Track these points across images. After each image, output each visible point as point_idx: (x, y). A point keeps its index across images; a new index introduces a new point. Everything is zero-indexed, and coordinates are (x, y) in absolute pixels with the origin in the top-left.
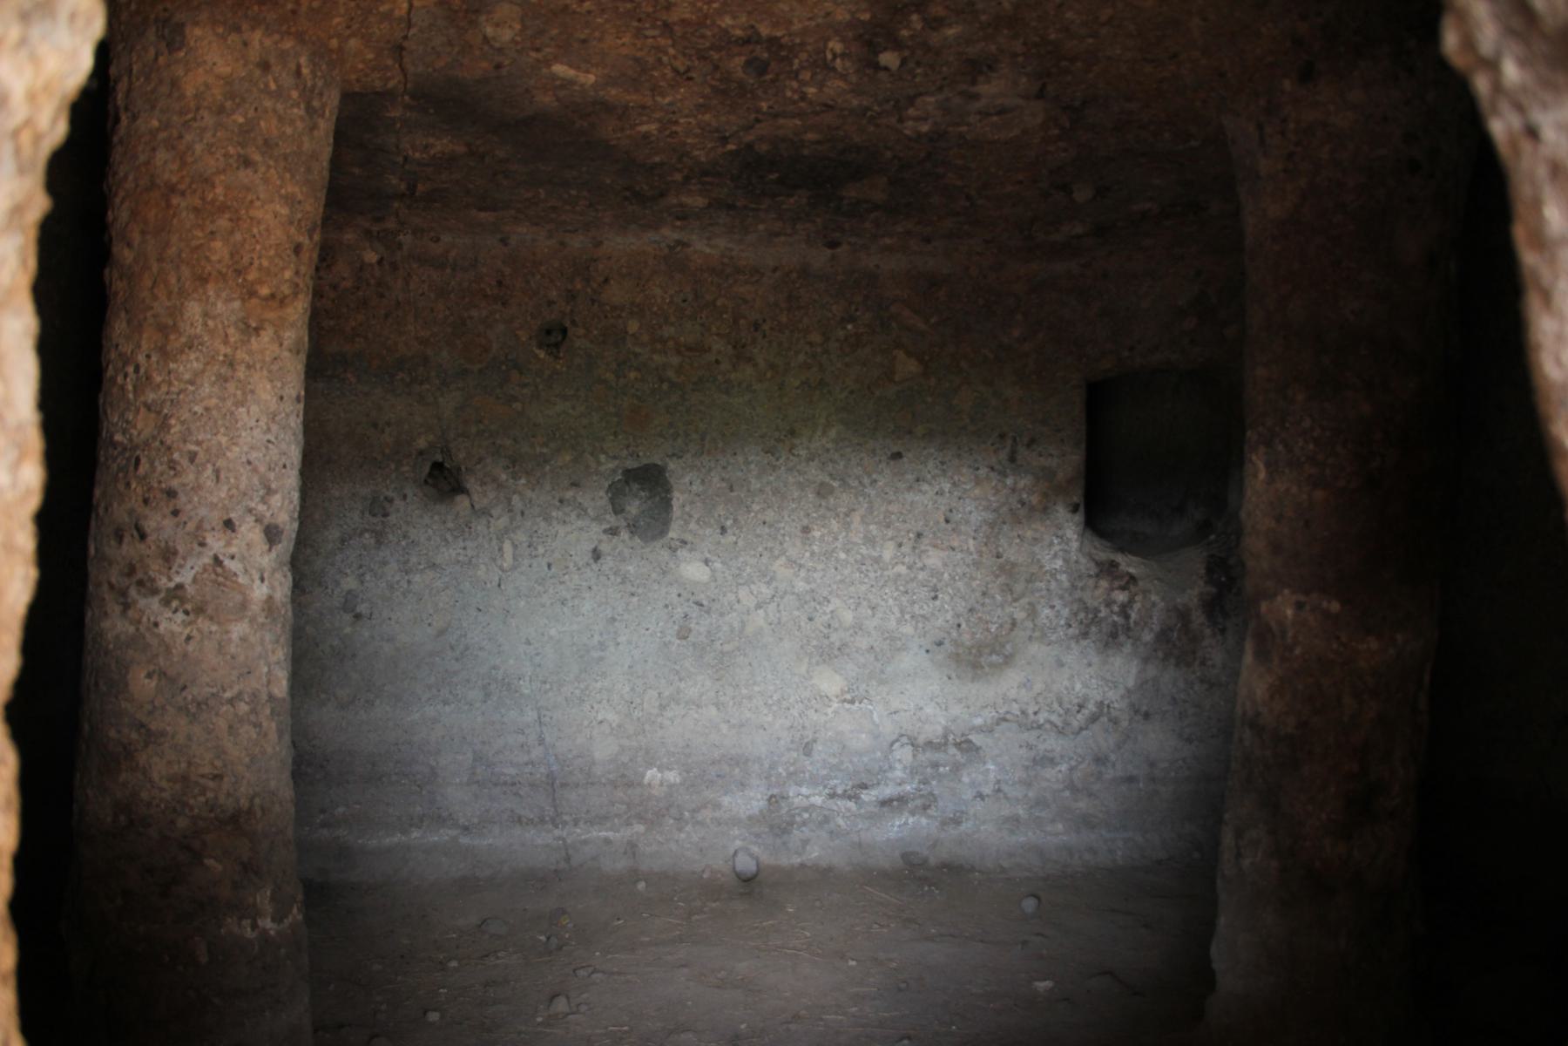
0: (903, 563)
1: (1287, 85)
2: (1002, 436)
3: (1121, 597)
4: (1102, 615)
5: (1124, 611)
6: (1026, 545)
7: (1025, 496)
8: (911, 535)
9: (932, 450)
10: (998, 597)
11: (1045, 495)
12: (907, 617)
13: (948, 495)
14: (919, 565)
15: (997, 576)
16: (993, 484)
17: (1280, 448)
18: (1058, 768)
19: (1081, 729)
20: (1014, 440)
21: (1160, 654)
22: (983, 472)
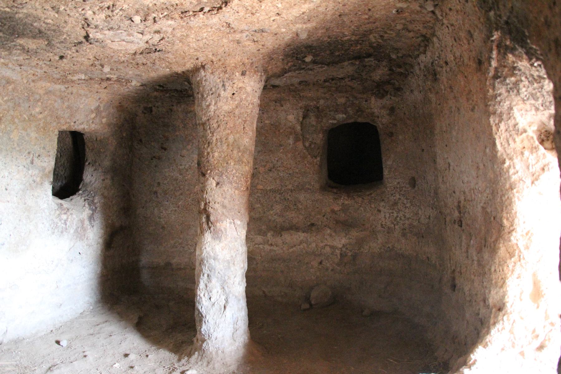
2: (29, 153)
3: (64, 217)
5: (66, 221)
6: (35, 198)
7: (35, 178)
10: (24, 221)
11: (41, 178)
13: (7, 178)
15: (24, 213)
16: (24, 173)
17: (225, 178)
20: (33, 154)
21: (75, 237)
22: (21, 168)
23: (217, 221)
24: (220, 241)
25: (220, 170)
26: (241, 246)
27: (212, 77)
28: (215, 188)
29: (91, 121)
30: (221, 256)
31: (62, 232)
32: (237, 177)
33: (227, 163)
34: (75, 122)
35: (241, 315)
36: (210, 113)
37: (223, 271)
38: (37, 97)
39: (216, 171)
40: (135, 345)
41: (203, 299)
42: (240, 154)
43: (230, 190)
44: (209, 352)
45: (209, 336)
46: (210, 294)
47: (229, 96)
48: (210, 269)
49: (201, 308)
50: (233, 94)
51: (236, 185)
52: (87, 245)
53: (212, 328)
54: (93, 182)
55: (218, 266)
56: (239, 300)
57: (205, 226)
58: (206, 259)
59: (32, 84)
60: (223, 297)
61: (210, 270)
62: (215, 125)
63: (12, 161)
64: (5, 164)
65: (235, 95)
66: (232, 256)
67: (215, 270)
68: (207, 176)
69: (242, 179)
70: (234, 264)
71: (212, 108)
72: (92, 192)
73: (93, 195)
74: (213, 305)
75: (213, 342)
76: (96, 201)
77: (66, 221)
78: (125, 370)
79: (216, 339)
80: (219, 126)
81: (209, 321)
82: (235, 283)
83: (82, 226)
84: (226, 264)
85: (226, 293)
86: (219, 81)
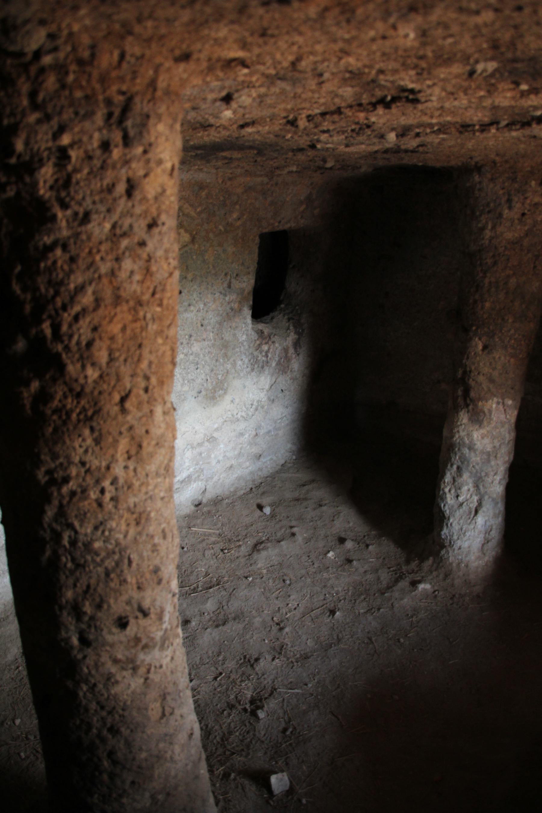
0: (183, 353)
1: (533, 183)
2: (226, 274)
3: (265, 347)
4: (259, 358)
5: (267, 352)
7: (233, 305)
8: (187, 337)
9: (195, 287)
10: (221, 360)
11: (240, 302)
12: (186, 382)
14: (190, 352)
15: (221, 350)
16: (221, 301)
17: (497, 340)
18: (245, 437)
19: (253, 415)
21: (277, 370)
22: (217, 295)
23: (480, 399)
24: (480, 426)
25: (491, 327)
26: (509, 433)
27: (491, 185)
28: (480, 353)
29: (300, 217)
30: (479, 445)
31: (263, 367)
32: (515, 339)
33: (503, 319)
34: (280, 222)
35: (497, 522)
36: (483, 242)
37: (480, 465)
38: (235, 198)
39: (486, 329)
40: (351, 524)
41: (448, 496)
42: (524, 306)
43: (503, 358)
44: (448, 563)
45: (450, 543)
46: (459, 491)
47: (516, 217)
48: (463, 460)
49: (444, 505)
50: (523, 214)
51: (512, 351)
52: (291, 379)
53: (455, 534)
54: (299, 293)
55: (475, 459)
56: (497, 503)
57: (460, 401)
58: (458, 445)
59: (229, 183)
60: (475, 498)
61: (461, 461)
62: (490, 261)
63: (207, 288)
64: (200, 293)
65: (526, 217)
66: (495, 447)
67: (468, 462)
68: (471, 334)
69: (523, 342)
70: (496, 457)
71: (488, 233)
72: (297, 308)
73: (299, 312)
74: (461, 505)
75: (456, 552)
76: (303, 321)
77: (267, 352)
78: (342, 563)
79: (460, 548)
80: (495, 263)
81: (454, 525)
82: (494, 482)
83: (286, 355)
84: (485, 457)
85: (480, 493)
86: (501, 192)
